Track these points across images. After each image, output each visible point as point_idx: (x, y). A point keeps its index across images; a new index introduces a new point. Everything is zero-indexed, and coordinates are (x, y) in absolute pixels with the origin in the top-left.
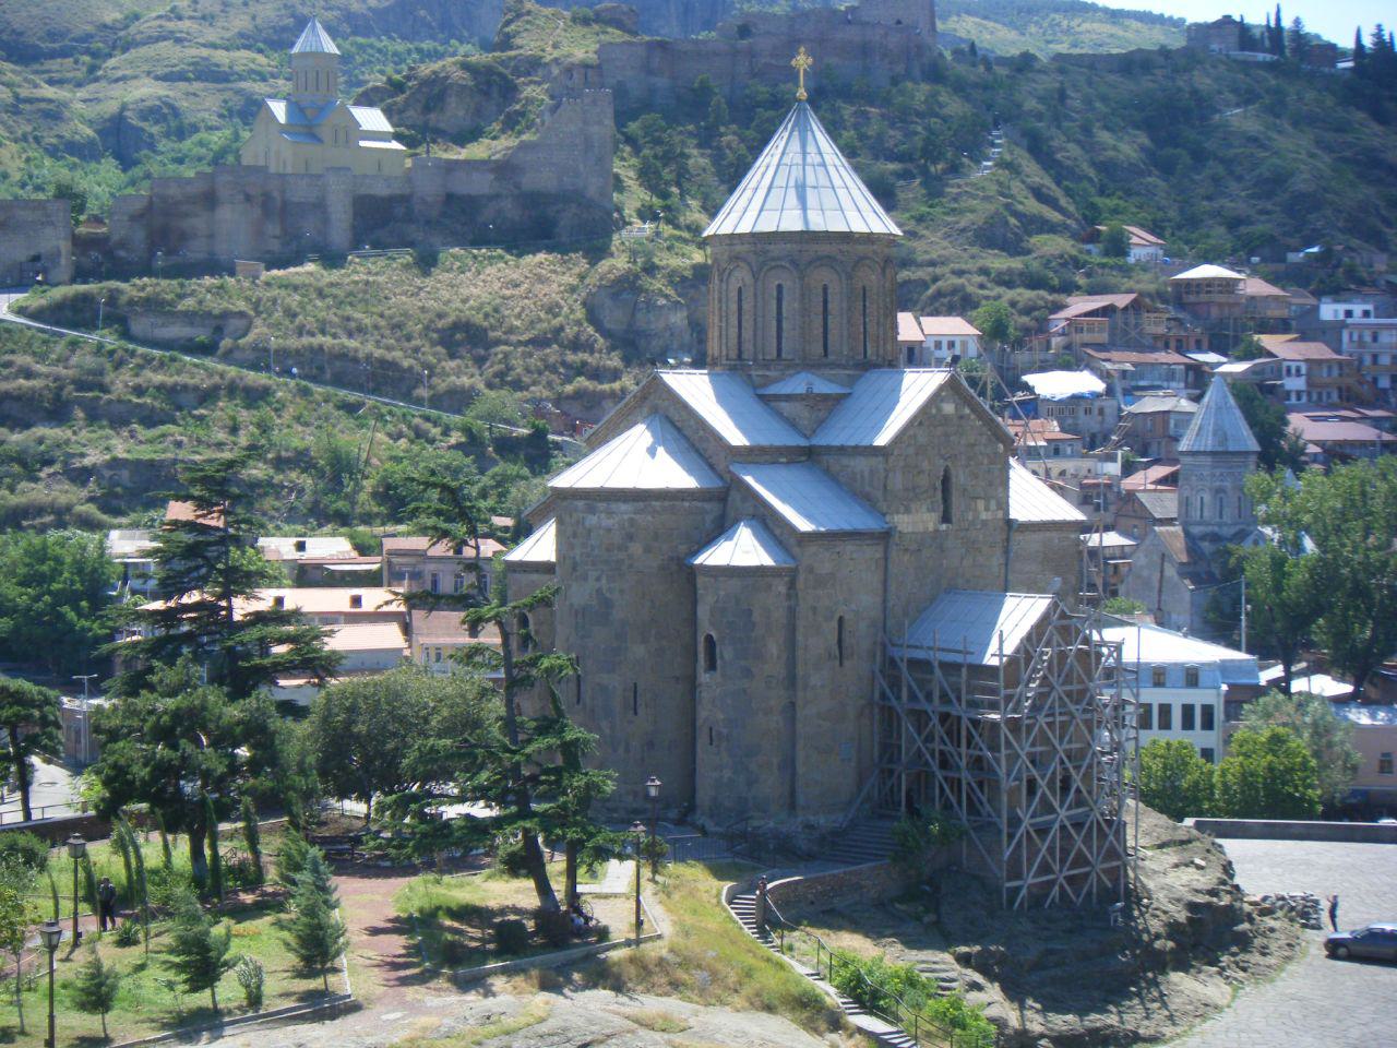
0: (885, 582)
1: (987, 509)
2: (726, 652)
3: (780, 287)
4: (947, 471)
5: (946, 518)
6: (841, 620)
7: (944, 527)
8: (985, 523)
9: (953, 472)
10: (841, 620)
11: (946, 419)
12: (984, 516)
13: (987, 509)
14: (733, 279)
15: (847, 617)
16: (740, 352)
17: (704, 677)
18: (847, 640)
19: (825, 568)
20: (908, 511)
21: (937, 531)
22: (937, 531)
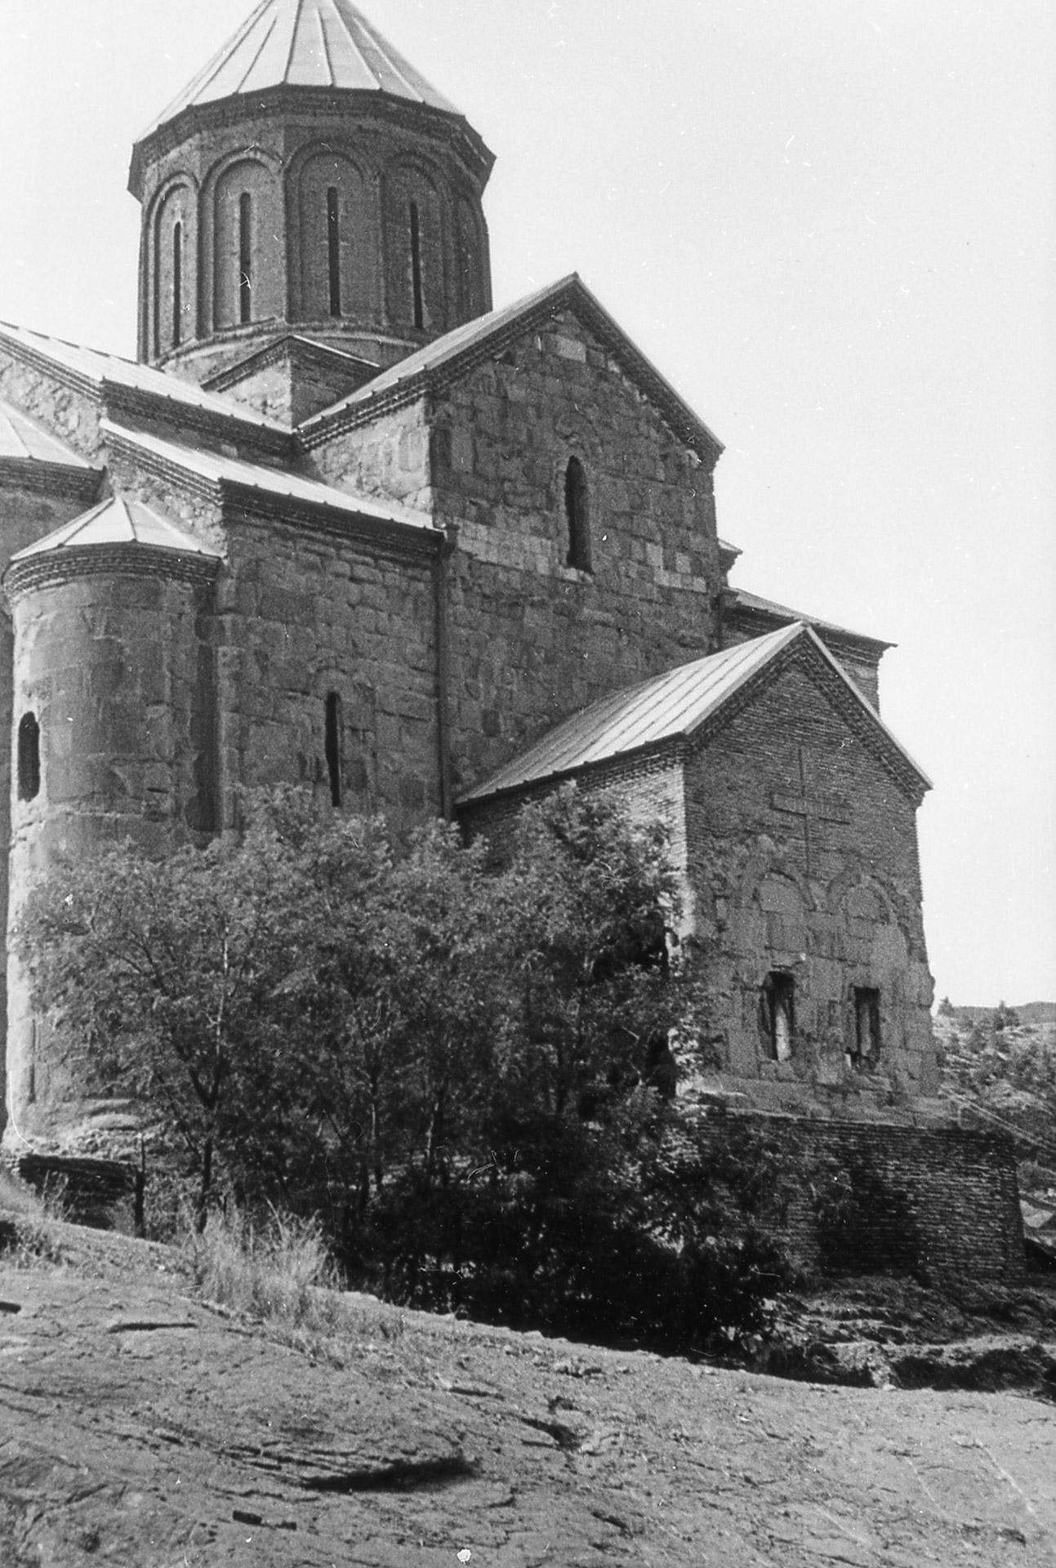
0: (437, 646)
1: (670, 566)
2: (55, 741)
3: (245, 199)
4: (574, 461)
5: (577, 556)
6: (332, 700)
7: (572, 574)
8: (668, 594)
9: (590, 471)
10: (332, 700)
11: (567, 369)
12: (664, 579)
13: (670, 566)
14: (167, 212)
15: (345, 699)
16: (177, 333)
17: (20, 810)
18: (348, 746)
19: (289, 575)
20: (484, 519)
21: (555, 579)
22: (555, 579)
